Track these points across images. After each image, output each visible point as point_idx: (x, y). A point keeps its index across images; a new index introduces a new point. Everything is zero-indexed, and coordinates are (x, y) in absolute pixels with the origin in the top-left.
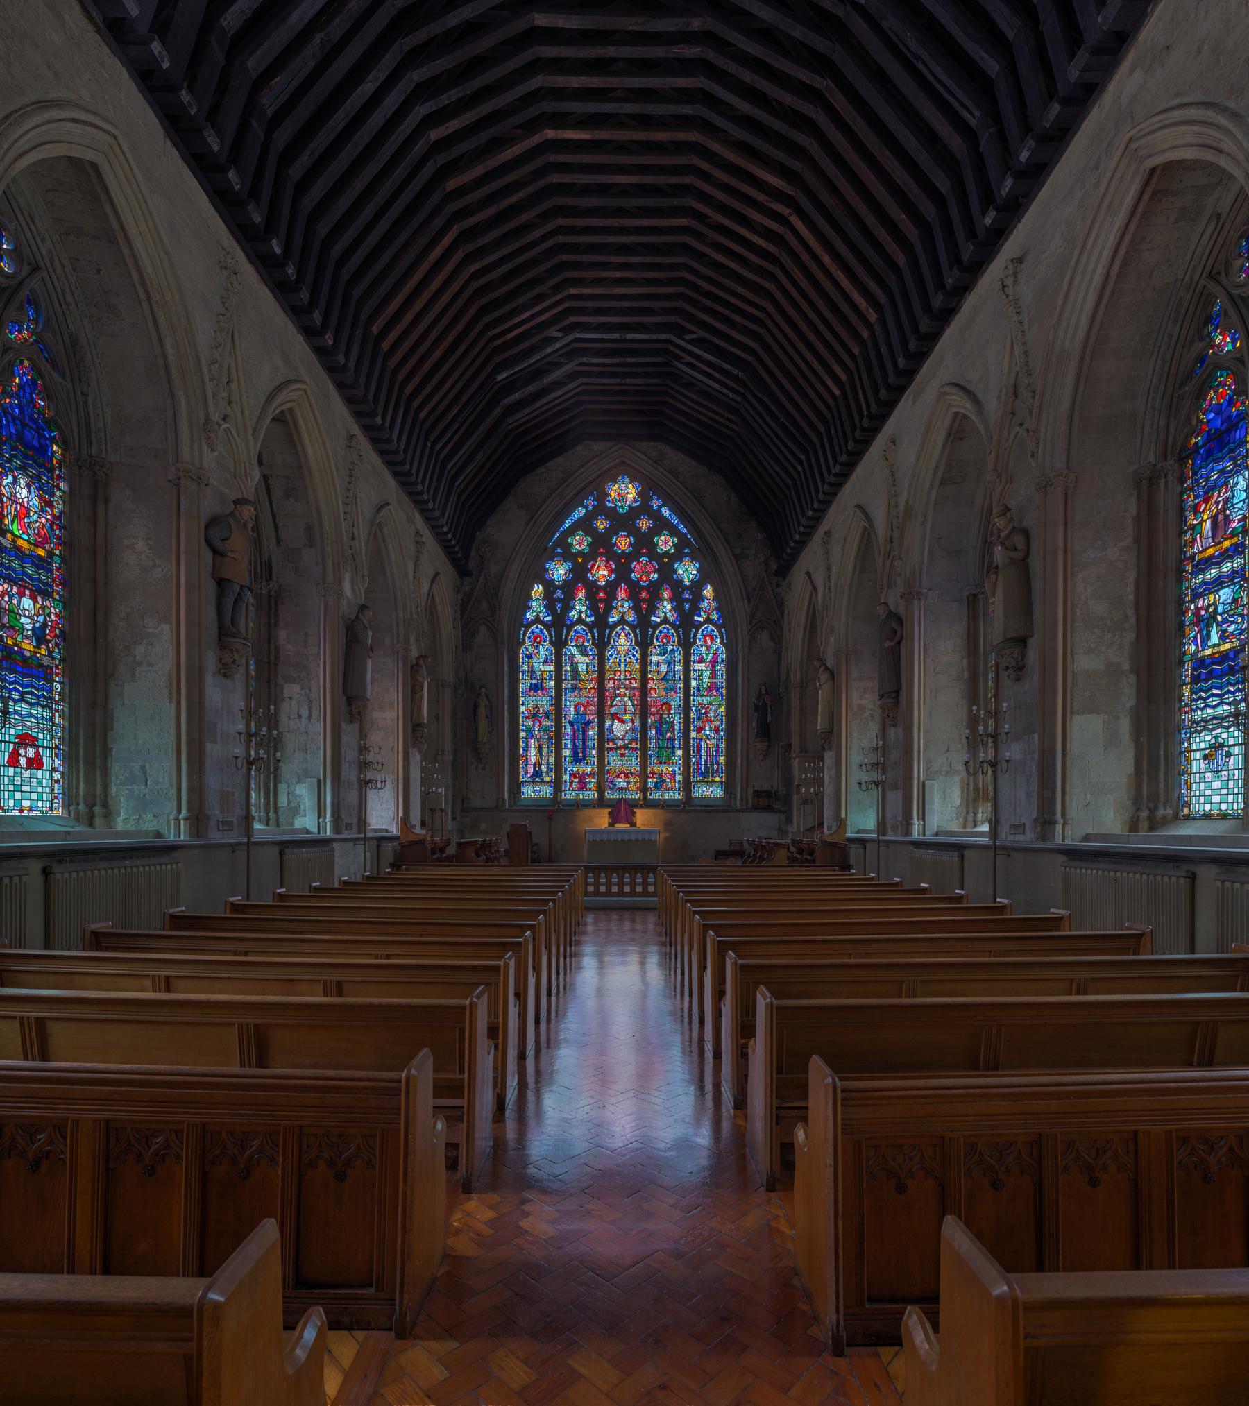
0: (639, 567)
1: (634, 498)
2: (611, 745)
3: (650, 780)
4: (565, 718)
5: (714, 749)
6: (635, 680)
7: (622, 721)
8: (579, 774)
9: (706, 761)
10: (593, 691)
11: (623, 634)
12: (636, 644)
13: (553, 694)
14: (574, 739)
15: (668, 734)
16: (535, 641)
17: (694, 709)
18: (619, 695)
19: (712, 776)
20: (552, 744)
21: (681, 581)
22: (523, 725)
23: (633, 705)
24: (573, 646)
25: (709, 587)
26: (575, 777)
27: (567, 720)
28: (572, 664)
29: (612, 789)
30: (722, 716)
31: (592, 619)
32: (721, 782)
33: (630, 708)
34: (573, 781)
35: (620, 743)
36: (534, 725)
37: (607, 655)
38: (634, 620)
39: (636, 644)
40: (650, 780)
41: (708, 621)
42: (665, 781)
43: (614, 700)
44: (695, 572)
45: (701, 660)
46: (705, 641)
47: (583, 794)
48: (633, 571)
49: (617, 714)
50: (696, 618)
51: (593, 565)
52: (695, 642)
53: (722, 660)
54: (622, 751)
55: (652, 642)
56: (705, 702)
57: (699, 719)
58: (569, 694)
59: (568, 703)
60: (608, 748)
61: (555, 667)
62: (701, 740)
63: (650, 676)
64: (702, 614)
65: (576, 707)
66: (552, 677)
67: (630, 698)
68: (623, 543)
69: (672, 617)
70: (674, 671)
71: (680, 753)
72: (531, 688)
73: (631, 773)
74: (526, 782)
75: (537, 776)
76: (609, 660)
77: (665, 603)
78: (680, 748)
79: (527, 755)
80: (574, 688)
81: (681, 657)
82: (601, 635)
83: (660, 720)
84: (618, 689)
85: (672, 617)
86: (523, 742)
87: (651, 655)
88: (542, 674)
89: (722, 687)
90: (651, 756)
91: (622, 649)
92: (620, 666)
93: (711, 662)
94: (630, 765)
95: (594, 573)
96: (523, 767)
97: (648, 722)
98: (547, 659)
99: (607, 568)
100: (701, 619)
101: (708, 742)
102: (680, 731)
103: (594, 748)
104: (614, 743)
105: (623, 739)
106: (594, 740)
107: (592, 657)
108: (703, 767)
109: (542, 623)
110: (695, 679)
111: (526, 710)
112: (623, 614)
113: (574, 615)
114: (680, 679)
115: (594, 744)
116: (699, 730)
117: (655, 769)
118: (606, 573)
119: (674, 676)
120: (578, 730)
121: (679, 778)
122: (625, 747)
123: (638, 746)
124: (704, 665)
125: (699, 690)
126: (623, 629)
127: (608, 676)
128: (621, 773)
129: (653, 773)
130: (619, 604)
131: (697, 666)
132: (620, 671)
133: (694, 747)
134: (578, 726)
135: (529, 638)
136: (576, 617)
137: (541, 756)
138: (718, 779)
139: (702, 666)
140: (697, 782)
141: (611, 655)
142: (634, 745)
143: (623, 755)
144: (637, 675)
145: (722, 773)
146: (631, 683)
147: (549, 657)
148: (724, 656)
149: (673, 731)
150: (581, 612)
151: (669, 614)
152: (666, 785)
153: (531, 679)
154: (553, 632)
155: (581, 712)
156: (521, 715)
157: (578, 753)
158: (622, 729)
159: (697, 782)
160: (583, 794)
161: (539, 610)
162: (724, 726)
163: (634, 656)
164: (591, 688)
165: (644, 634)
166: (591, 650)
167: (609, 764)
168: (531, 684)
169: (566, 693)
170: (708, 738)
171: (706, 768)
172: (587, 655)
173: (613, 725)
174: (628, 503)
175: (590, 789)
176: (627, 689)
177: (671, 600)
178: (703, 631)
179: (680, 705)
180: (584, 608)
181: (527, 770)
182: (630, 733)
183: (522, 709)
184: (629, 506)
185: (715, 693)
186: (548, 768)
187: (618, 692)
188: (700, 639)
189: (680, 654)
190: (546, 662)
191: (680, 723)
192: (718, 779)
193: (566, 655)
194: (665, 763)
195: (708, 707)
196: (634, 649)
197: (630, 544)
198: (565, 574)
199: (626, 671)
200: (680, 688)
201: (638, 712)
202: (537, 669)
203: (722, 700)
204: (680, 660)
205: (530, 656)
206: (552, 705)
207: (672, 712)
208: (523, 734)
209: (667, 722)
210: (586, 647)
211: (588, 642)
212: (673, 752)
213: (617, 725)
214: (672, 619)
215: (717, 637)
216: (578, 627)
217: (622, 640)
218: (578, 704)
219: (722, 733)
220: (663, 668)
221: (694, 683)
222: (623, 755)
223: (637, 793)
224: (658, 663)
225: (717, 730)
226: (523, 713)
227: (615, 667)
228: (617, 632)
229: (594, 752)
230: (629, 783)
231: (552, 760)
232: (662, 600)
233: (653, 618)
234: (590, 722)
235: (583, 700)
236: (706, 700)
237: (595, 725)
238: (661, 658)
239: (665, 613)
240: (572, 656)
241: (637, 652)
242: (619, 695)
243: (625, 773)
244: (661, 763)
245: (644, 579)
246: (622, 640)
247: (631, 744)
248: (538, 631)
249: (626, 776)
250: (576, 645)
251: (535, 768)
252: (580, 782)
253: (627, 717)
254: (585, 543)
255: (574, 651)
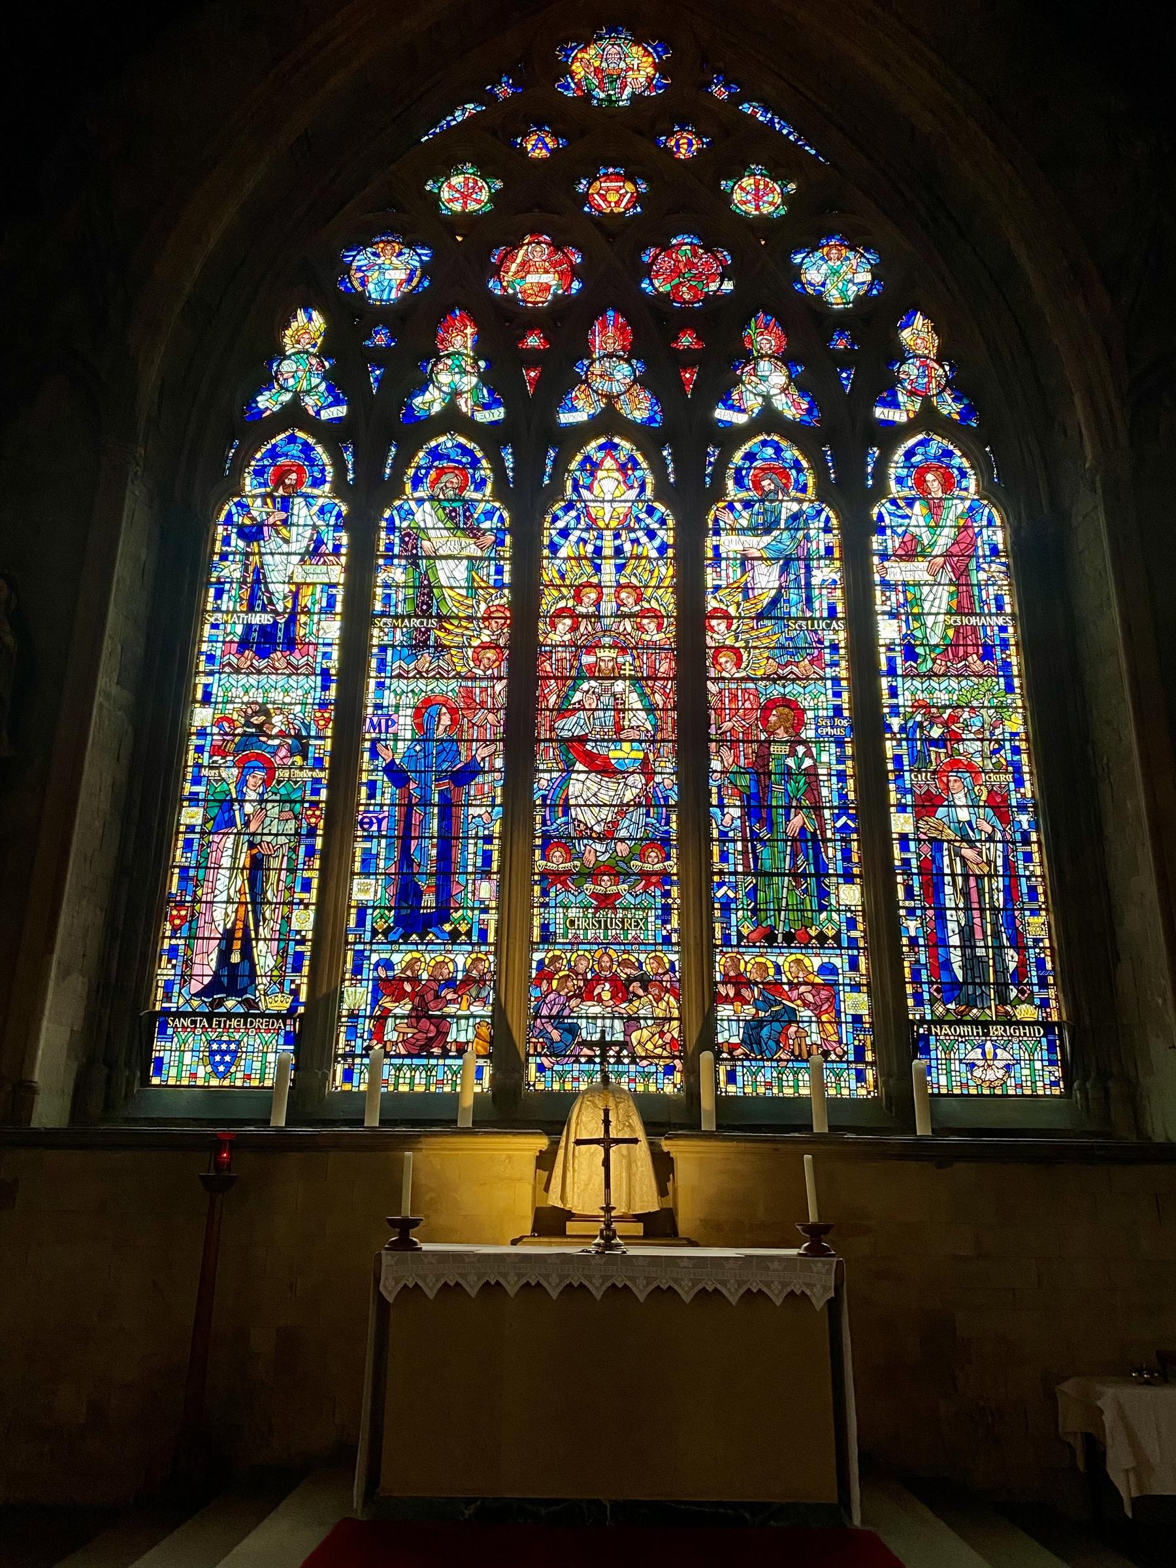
0: (665, 263)
1: (650, 79)
2: (557, 861)
3: (725, 1011)
4: (374, 754)
5: (1000, 883)
6: (656, 616)
7: (604, 768)
8: (415, 980)
9: (967, 934)
10: (491, 654)
11: (609, 463)
12: (658, 497)
13: (333, 665)
14: (406, 839)
15: (797, 821)
16: (279, 481)
17: (895, 723)
18: (593, 673)
19: (1003, 1000)
20: (310, 852)
21: (818, 301)
22: (196, 781)
23: (651, 709)
24: (420, 501)
25: (919, 320)
26: (399, 997)
27: (380, 763)
28: (414, 560)
29: (555, 1052)
30: (1016, 751)
31: (498, 414)
32: (1048, 1026)
33: (640, 719)
34: (386, 1014)
35: (595, 852)
36: (242, 782)
37: (550, 533)
38: (652, 419)
39: (658, 497)
40: (725, 1011)
41: (928, 419)
42: (791, 1017)
43: (574, 689)
44: (868, 277)
45: (911, 552)
46: (920, 482)
47: (428, 1069)
48: (647, 271)
49: (583, 740)
50: (880, 413)
51: (508, 256)
52: (880, 490)
53: (994, 551)
54: (606, 885)
55: (718, 492)
56: (943, 698)
57: (919, 760)
58: (395, 665)
59: (388, 699)
60: (544, 875)
61: (348, 569)
62: (936, 844)
63: (712, 604)
64: (902, 398)
65: (418, 713)
66: (331, 604)
67: (635, 680)
68: (612, 197)
69: (790, 407)
70: (808, 585)
71: (850, 895)
72: (244, 644)
73: (645, 982)
74: (179, 1014)
75: (232, 991)
76: (554, 548)
77: (764, 366)
78: (848, 878)
79: (196, 900)
80: (419, 644)
81: (833, 539)
82: (529, 465)
83: (760, 769)
84: (590, 649)
85: (790, 407)
86: (188, 844)
87: (717, 533)
88: (295, 596)
89: (1005, 644)
90: (726, 907)
91: (605, 514)
92: (598, 569)
93: (947, 555)
94: (637, 942)
95: (508, 277)
96: (174, 950)
97: (706, 771)
98: (319, 542)
99: (554, 265)
100: (899, 417)
101: (968, 853)
102: (843, 809)
103: (484, 872)
104: (570, 855)
105: (608, 836)
106: (488, 840)
107: (490, 538)
108: (956, 957)
109: (312, 424)
110: (893, 615)
111: (217, 723)
112: (610, 398)
113: (430, 401)
114: (832, 610)
115: (487, 858)
116: (926, 805)
117: (749, 962)
118: (551, 279)
119: (809, 600)
120: (425, 803)
121: (856, 1003)
122: (616, 872)
123: (672, 866)
124: (921, 565)
125: (910, 653)
126: (609, 447)
127: (549, 602)
128: (598, 979)
129: (739, 981)
130: (597, 368)
131: (897, 572)
132: (599, 587)
133: (908, 873)
134: (424, 788)
135: (259, 472)
136: (436, 408)
137: (257, 899)
138: (1026, 1012)
139: (917, 571)
140: (940, 1022)
141: (564, 533)
142: (653, 863)
143: (606, 901)
144: (666, 601)
145: (1043, 984)
146: (640, 628)
147: (329, 537)
148: (999, 538)
149: (817, 808)
150: (456, 393)
151: (780, 402)
152: (801, 1036)
153: (251, 609)
154: (348, 457)
155: (440, 733)
156: (195, 741)
157: (419, 894)
158: (604, 797)
159: (940, 1022)
160: (428, 1069)
161: (305, 385)
162: (1027, 789)
163: (651, 535)
164: (484, 647)
165: (690, 464)
166: (489, 515)
167: (547, 937)
168: (248, 628)
169: (382, 664)
170: (965, 839)
171: (972, 962)
172: (474, 532)
173: (565, 781)
174: (628, 91)
175: (461, 1049)
176: (623, 650)
177: (786, 359)
178: (909, 454)
179: (838, 711)
180: (469, 382)
181: (188, 963)
182: (638, 815)
183: (202, 716)
184: (634, 97)
185: (978, 666)
186: (283, 953)
187: (587, 659)
188: (900, 480)
189: (827, 530)
190: (315, 551)
191: (841, 776)
192: (1026, 1012)
193: (391, 529)
194: (789, 938)
195: (953, 719)
196: (650, 511)
197: (637, 199)
198: (409, 280)
199: (620, 587)
200: (834, 648)
201: (669, 733)
202: (273, 576)
203: (1010, 688)
204: (829, 550)
205: (253, 533)
206: (323, 705)
207: (809, 733)
208: (191, 816)
209: (788, 773)
210: (469, 505)
211: (480, 485)
212: (823, 894)
213: (582, 785)
214: (790, 413)
215: (963, 474)
216: (444, 442)
217: (608, 483)
218: (428, 703)
219: (1024, 819)
220: (767, 579)
221: (888, 631)
222: (606, 901)
223: (670, 1070)
224: (745, 560)
225: (999, 806)
226: (202, 733)
227: (582, 573)
228: (588, 459)
229: (486, 890)
230: (632, 1022)
231: (304, 921)
232: (748, 357)
233: (721, 414)
234: (470, 772)
235: (450, 688)
236: (943, 692)
237: (491, 783)
238: (755, 544)
239: (767, 398)
240: (412, 538)
241: (663, 522)
242: (593, 673)
243: (614, 980)
244: (770, 938)
245: (687, 297)
246: (608, 483)
247: (642, 857)
248: (295, 450)
249: (621, 990)
250: (432, 498)
251: (224, 955)
252: (419, 1015)
253: (624, 753)
254: (484, 196)
255: (425, 515)
